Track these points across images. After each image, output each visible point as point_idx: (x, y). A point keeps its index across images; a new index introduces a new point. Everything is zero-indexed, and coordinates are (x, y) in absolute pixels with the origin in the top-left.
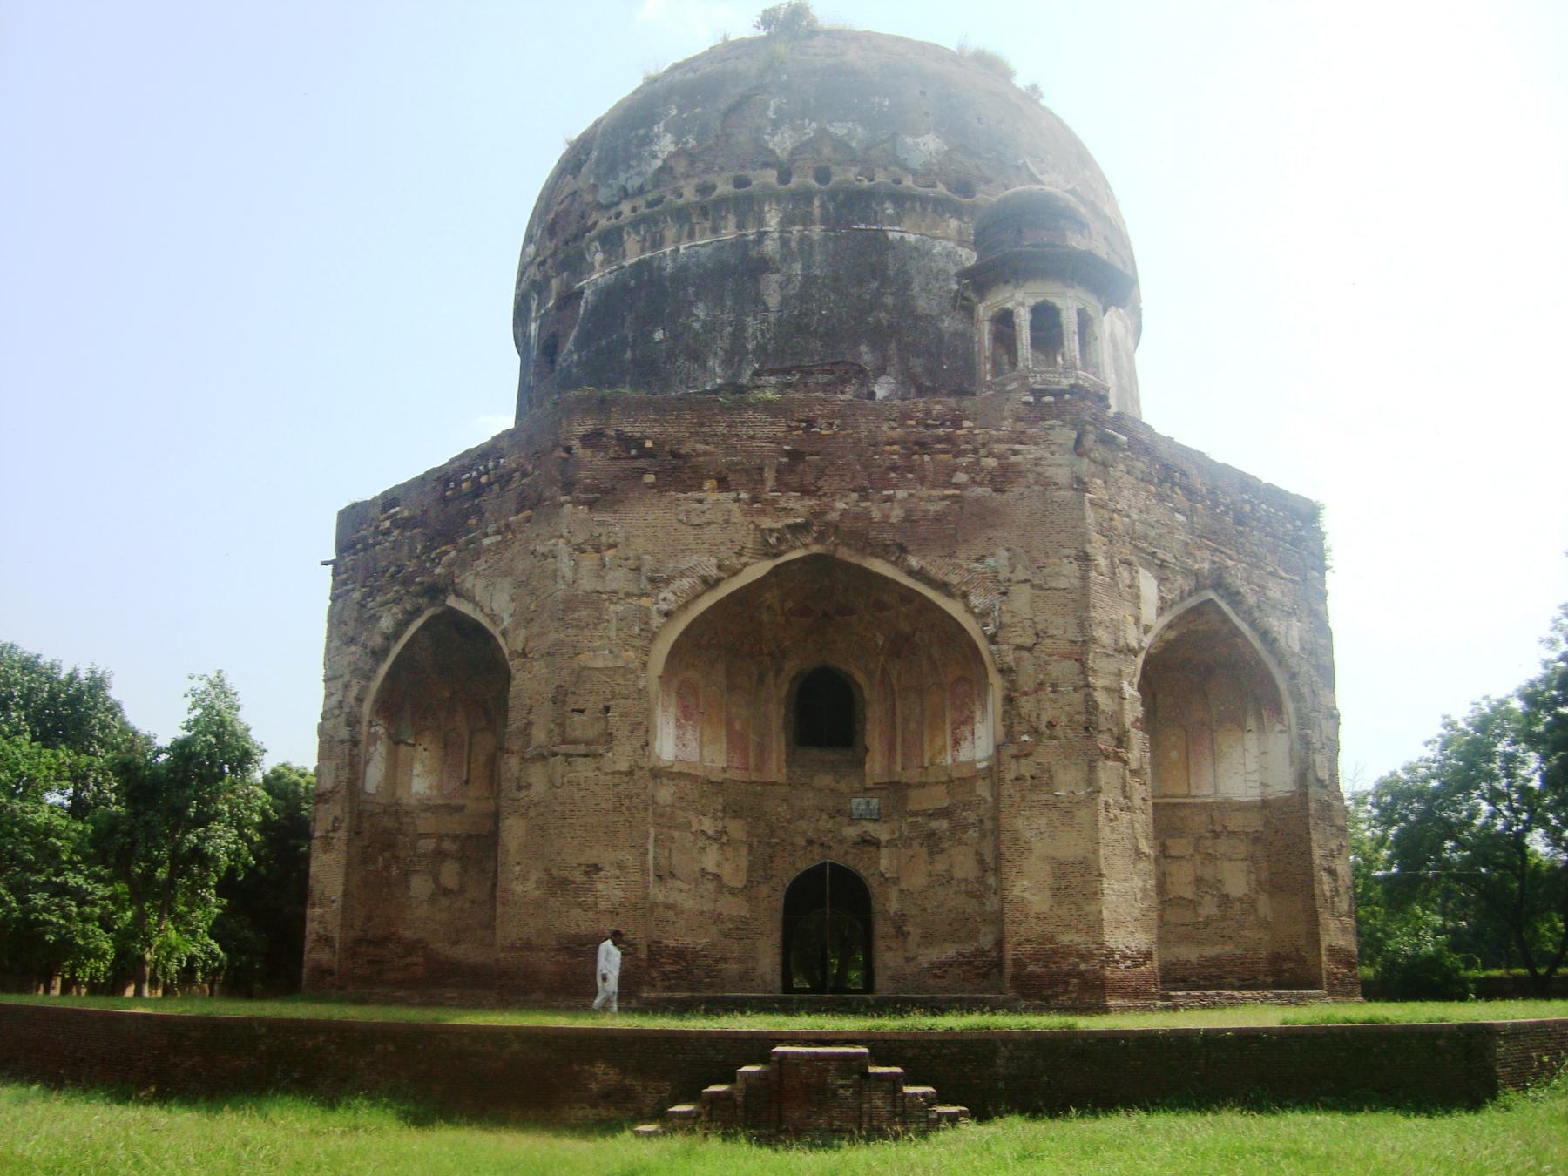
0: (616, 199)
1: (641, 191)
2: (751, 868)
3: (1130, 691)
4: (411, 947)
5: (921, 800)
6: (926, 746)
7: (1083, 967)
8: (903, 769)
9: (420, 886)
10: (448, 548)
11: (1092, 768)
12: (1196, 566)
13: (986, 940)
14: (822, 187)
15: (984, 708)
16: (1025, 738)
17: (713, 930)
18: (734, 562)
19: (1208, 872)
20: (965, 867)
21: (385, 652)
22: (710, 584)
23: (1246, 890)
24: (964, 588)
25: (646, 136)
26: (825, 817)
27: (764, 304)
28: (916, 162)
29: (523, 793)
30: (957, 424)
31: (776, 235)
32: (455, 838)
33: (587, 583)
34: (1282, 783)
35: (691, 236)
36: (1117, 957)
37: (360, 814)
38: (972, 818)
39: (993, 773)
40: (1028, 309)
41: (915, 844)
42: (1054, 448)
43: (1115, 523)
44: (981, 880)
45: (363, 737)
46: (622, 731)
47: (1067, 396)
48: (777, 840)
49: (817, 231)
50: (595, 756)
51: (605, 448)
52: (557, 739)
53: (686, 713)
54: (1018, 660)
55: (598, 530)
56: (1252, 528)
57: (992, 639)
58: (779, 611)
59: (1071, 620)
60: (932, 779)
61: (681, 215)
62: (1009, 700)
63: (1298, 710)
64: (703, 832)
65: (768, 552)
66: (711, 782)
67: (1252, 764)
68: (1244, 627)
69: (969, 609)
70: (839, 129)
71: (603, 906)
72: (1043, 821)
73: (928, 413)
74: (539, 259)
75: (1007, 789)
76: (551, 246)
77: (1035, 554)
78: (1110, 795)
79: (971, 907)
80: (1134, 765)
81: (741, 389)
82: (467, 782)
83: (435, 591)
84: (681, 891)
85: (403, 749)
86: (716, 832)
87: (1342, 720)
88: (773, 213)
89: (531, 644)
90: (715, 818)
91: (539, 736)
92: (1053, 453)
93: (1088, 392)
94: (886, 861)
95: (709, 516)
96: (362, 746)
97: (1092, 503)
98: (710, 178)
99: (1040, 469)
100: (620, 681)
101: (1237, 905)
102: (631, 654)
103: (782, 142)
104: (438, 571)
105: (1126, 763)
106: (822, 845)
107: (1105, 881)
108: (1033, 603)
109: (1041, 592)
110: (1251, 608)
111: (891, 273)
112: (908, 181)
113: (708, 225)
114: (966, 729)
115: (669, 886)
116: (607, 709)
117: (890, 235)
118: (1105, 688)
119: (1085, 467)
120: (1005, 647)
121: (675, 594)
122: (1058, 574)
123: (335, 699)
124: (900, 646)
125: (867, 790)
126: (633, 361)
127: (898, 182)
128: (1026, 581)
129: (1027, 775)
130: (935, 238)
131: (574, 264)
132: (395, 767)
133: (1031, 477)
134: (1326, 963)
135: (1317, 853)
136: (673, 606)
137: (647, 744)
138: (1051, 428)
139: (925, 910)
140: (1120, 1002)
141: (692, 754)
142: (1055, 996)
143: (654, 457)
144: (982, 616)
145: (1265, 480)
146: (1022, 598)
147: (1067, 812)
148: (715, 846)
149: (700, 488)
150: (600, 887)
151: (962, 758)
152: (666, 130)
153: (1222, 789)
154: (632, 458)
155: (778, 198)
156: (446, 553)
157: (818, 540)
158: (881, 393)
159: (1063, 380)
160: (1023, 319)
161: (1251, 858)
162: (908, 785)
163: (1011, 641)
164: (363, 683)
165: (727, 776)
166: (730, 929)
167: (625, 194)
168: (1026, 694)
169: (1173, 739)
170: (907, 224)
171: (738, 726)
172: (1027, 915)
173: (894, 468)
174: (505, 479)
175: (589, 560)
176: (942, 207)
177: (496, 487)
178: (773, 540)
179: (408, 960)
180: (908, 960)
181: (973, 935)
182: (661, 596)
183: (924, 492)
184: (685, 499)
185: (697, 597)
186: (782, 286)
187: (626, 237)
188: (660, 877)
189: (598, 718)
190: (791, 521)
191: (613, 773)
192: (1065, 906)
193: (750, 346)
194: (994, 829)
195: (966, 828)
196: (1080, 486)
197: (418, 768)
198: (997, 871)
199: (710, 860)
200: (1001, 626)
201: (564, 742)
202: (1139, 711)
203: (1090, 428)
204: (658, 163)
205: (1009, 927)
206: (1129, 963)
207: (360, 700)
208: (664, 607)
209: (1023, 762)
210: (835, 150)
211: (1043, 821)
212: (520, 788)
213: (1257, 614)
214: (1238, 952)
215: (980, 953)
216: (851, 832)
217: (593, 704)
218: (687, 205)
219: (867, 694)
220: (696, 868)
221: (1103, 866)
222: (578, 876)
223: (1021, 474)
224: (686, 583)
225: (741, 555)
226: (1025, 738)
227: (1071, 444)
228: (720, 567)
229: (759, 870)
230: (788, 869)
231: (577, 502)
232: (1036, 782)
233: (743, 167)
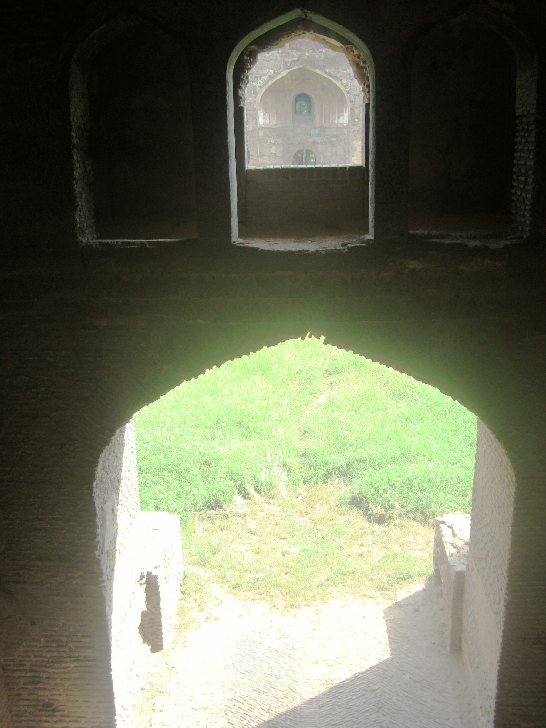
8: (325, 123)
15: (346, 109)
16: (356, 120)
22: (271, 78)
24: (341, 78)
38: (342, 139)
39: (348, 127)
53: (265, 111)
62: (352, 109)
64: (271, 143)
65: (287, 68)
66: (273, 129)
69: (342, 84)
84: (266, 159)
86: (274, 142)
100: (249, 106)
102: (251, 98)
106: (303, 143)
120: (351, 95)
121: (262, 81)
137: (257, 123)
141: (268, 123)
144: (346, 86)
157: (301, 64)
163: (353, 93)
168: (356, 108)
182: (259, 82)
185: (268, 81)
199: (273, 150)
200: (350, 89)
208: (260, 85)
209: (355, 126)
216: (310, 140)
224: (265, 78)
225: (280, 69)
226: (356, 120)
228: (274, 73)
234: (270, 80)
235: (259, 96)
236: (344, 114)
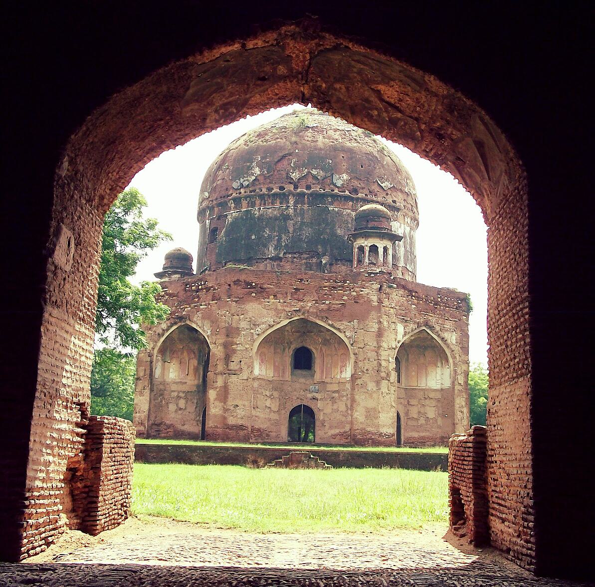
3: (393, 361)
5: (331, 388)
6: (332, 372)
7: (373, 437)
10: (188, 306)
13: (347, 428)
16: (360, 373)
17: (268, 423)
18: (278, 320)
22: (271, 326)
25: (250, 166)
27: (289, 231)
28: (339, 185)
31: (292, 207)
35: (265, 204)
36: (383, 435)
38: (345, 394)
42: (373, 290)
49: (306, 206)
53: (262, 361)
55: (239, 309)
56: (440, 306)
61: (262, 197)
70: (314, 172)
71: (239, 416)
76: (215, 196)
78: (384, 389)
79: (344, 419)
81: (280, 259)
83: (181, 318)
90: (269, 391)
91: (220, 368)
98: (271, 185)
103: (295, 175)
104: (184, 313)
110: (437, 332)
112: (336, 191)
116: (241, 361)
117: (329, 208)
118: (384, 360)
124: (326, 342)
126: (245, 244)
131: (223, 205)
143: (254, 288)
147: (371, 396)
149: (268, 298)
154: (249, 288)
155: (294, 195)
158: (324, 262)
159: (377, 269)
160: (367, 249)
170: (335, 203)
171: (277, 364)
173: (325, 295)
174: (208, 289)
176: (347, 198)
177: (205, 290)
178: (290, 314)
181: (344, 427)
187: (242, 201)
195: (343, 396)
196: (380, 301)
199: (268, 403)
202: (394, 366)
204: (254, 178)
211: (363, 397)
212: (214, 382)
220: (265, 405)
222: (232, 408)
226: (360, 373)
229: (282, 406)
231: (232, 301)
235: (257, 344)
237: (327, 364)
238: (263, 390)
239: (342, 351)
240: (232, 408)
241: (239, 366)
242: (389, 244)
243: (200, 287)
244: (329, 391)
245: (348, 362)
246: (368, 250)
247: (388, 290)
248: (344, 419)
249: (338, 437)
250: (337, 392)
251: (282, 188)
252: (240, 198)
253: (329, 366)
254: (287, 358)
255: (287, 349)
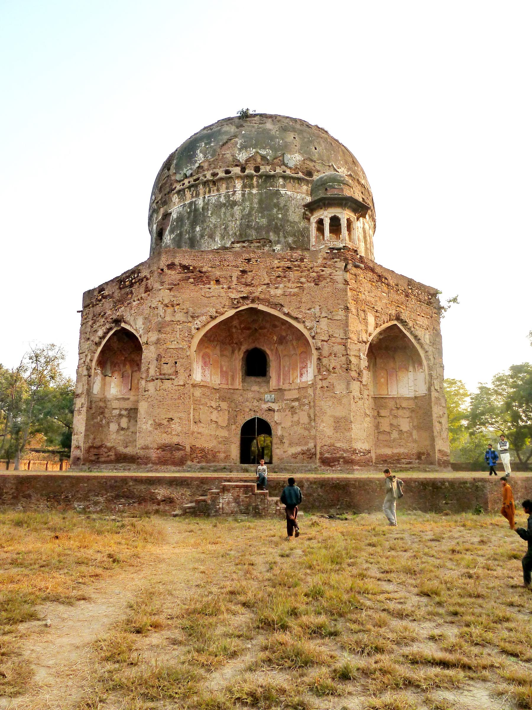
0: (182, 179)
1: (191, 175)
2: (229, 420)
3: (364, 357)
4: (110, 449)
7: (345, 455)
9: (113, 427)
10: (122, 306)
11: (348, 384)
12: (390, 312)
13: (311, 445)
14: (257, 174)
15: (311, 362)
16: (325, 373)
19: (395, 422)
20: (304, 419)
21: (100, 343)
23: (408, 429)
24: (303, 320)
26: (255, 401)
28: (291, 164)
29: (147, 393)
30: (302, 260)
31: (240, 192)
32: (126, 409)
33: (168, 319)
34: (422, 390)
35: (209, 192)
36: (357, 452)
37: (91, 402)
40: (328, 219)
41: (287, 411)
42: (337, 269)
43: (358, 296)
44: (309, 423)
45: (93, 374)
46: (181, 371)
47: (342, 250)
48: (237, 409)
50: (171, 379)
51: (175, 270)
52: (158, 374)
53: (205, 364)
54: (322, 345)
57: (313, 338)
58: (239, 328)
59: (342, 331)
60: (292, 388)
61: (205, 183)
62: (319, 359)
63: (428, 364)
67: (411, 383)
68: (408, 334)
69: (306, 327)
70: (263, 152)
71: (174, 433)
72: (330, 403)
73: (292, 256)
74: (156, 201)
75: (318, 391)
77: (329, 307)
78: (356, 393)
79: (306, 433)
80: (364, 383)
82: (130, 389)
83: (117, 322)
85: (107, 377)
87: (445, 368)
88: (239, 184)
89: (149, 340)
91: (152, 372)
92: (336, 271)
93: (350, 248)
94: (277, 417)
95: (212, 294)
96: (92, 377)
97: (350, 289)
98: (216, 171)
99: (331, 277)
101: (405, 434)
103: (242, 157)
105: (361, 382)
107: (353, 426)
108: (328, 325)
109: (330, 321)
111: (282, 205)
112: (288, 172)
113: (215, 188)
114: (305, 370)
115: (199, 425)
116: (176, 363)
119: (348, 276)
122: (337, 315)
123: (82, 361)
124: (282, 340)
125: (271, 391)
127: (284, 172)
128: (326, 317)
129: (325, 386)
130: (298, 193)
132: (104, 384)
133: (328, 280)
134: (437, 455)
135: (435, 416)
136: (200, 326)
138: (336, 262)
139: (290, 434)
140: (358, 468)
142: (335, 465)
143: (193, 272)
145: (417, 281)
146: (324, 323)
148: (216, 412)
149: (209, 283)
150: (173, 426)
151: (303, 380)
152: (201, 152)
153: (400, 392)
154: (186, 273)
156: (121, 307)
161: (411, 417)
162: (285, 390)
163: (320, 338)
164: (92, 354)
165: (220, 386)
166: (221, 441)
167: (186, 177)
168: (325, 357)
169: (382, 374)
171: (224, 369)
172: (325, 436)
173: (279, 277)
175: (170, 310)
177: (138, 284)
179: (109, 453)
180: (284, 452)
181: (306, 443)
183: (290, 285)
184: (204, 288)
185: (208, 323)
186: (242, 211)
188: (195, 422)
189: (172, 366)
190: (242, 296)
191: (178, 385)
192: (338, 433)
193: (231, 233)
194: (313, 405)
195: (304, 405)
197: (113, 385)
198: (315, 420)
201: (160, 374)
202: (366, 364)
203: (350, 262)
205: (318, 441)
206: (362, 454)
207: (91, 360)
208: (197, 327)
209: (324, 381)
210: (261, 159)
211: (330, 403)
212: (145, 391)
213: (412, 329)
214: (406, 451)
215: (309, 450)
216: (265, 406)
217: (171, 361)
218: (208, 181)
219: (270, 357)
220: (209, 419)
221: (352, 419)
222: (165, 422)
223: (325, 279)
224: (204, 318)
226: (325, 373)
227: (343, 267)
228: (216, 312)
229: (232, 420)
230: (242, 421)
232: (328, 389)
233: (228, 167)
234: (211, 321)
236: (309, 369)
237: (284, 367)
238: (207, 400)
239: (302, 349)
240: (165, 422)
241: (173, 369)
242: (352, 216)
243: (133, 281)
244: (287, 400)
245: (309, 361)
246: (329, 221)
247: (354, 269)
248: (306, 433)
249: (301, 456)
250: (297, 400)
251: (227, 172)
252: (183, 190)
253: (286, 369)
254: (237, 362)
255: (236, 352)
